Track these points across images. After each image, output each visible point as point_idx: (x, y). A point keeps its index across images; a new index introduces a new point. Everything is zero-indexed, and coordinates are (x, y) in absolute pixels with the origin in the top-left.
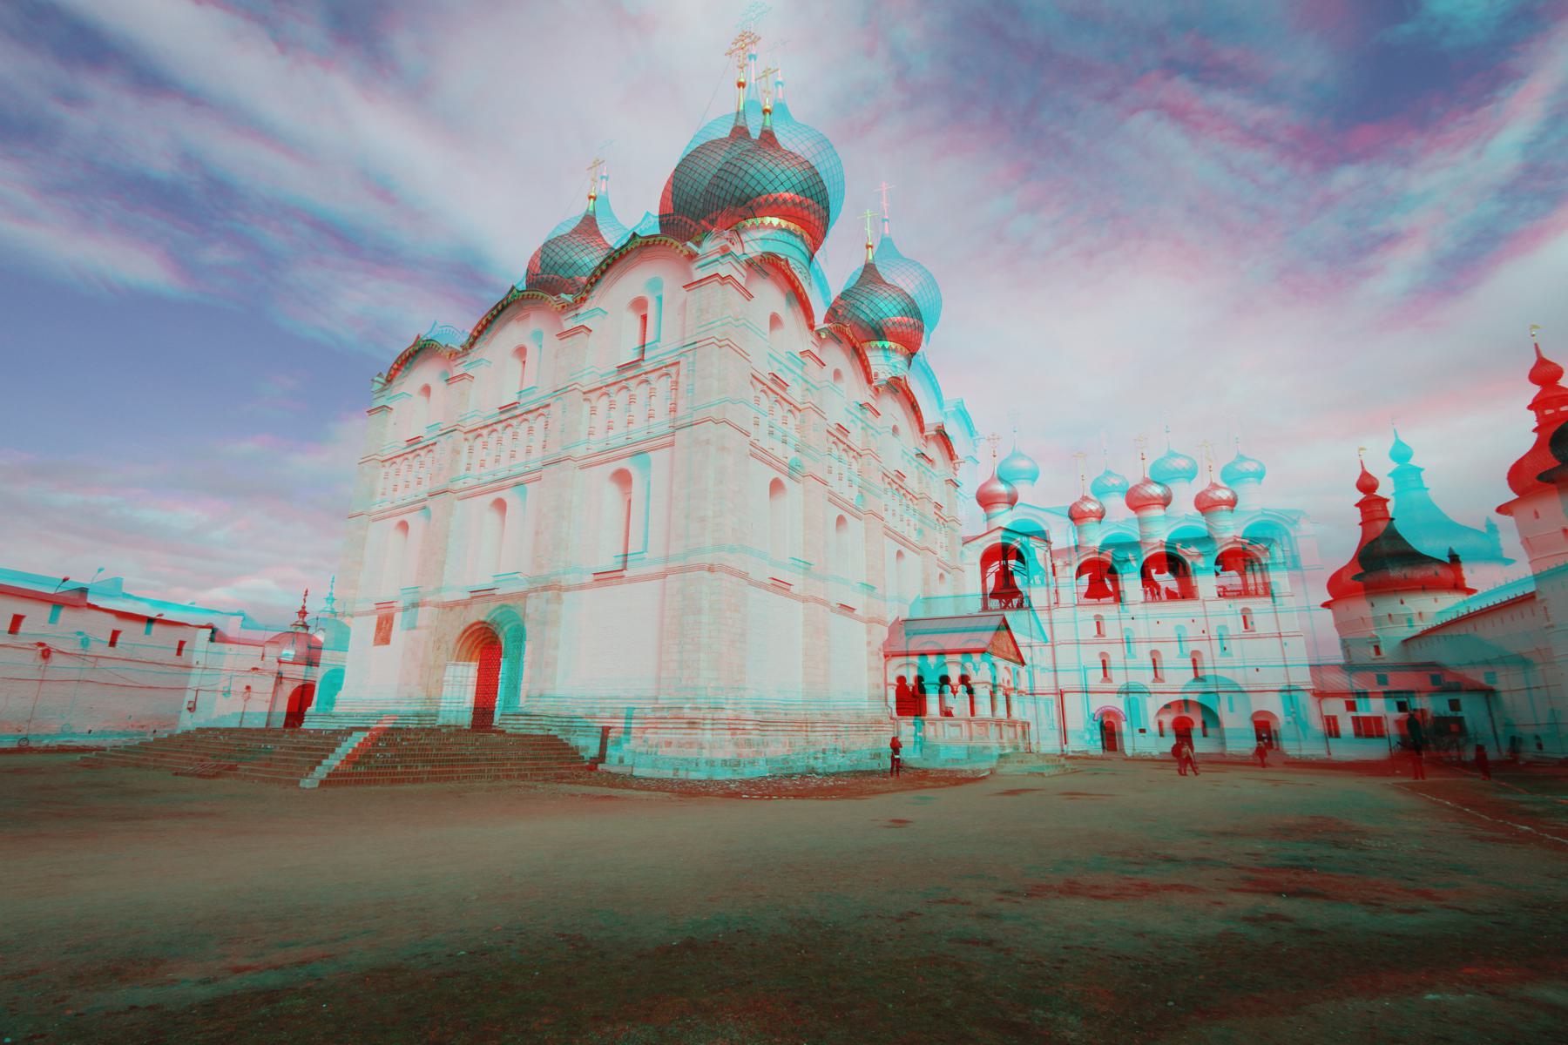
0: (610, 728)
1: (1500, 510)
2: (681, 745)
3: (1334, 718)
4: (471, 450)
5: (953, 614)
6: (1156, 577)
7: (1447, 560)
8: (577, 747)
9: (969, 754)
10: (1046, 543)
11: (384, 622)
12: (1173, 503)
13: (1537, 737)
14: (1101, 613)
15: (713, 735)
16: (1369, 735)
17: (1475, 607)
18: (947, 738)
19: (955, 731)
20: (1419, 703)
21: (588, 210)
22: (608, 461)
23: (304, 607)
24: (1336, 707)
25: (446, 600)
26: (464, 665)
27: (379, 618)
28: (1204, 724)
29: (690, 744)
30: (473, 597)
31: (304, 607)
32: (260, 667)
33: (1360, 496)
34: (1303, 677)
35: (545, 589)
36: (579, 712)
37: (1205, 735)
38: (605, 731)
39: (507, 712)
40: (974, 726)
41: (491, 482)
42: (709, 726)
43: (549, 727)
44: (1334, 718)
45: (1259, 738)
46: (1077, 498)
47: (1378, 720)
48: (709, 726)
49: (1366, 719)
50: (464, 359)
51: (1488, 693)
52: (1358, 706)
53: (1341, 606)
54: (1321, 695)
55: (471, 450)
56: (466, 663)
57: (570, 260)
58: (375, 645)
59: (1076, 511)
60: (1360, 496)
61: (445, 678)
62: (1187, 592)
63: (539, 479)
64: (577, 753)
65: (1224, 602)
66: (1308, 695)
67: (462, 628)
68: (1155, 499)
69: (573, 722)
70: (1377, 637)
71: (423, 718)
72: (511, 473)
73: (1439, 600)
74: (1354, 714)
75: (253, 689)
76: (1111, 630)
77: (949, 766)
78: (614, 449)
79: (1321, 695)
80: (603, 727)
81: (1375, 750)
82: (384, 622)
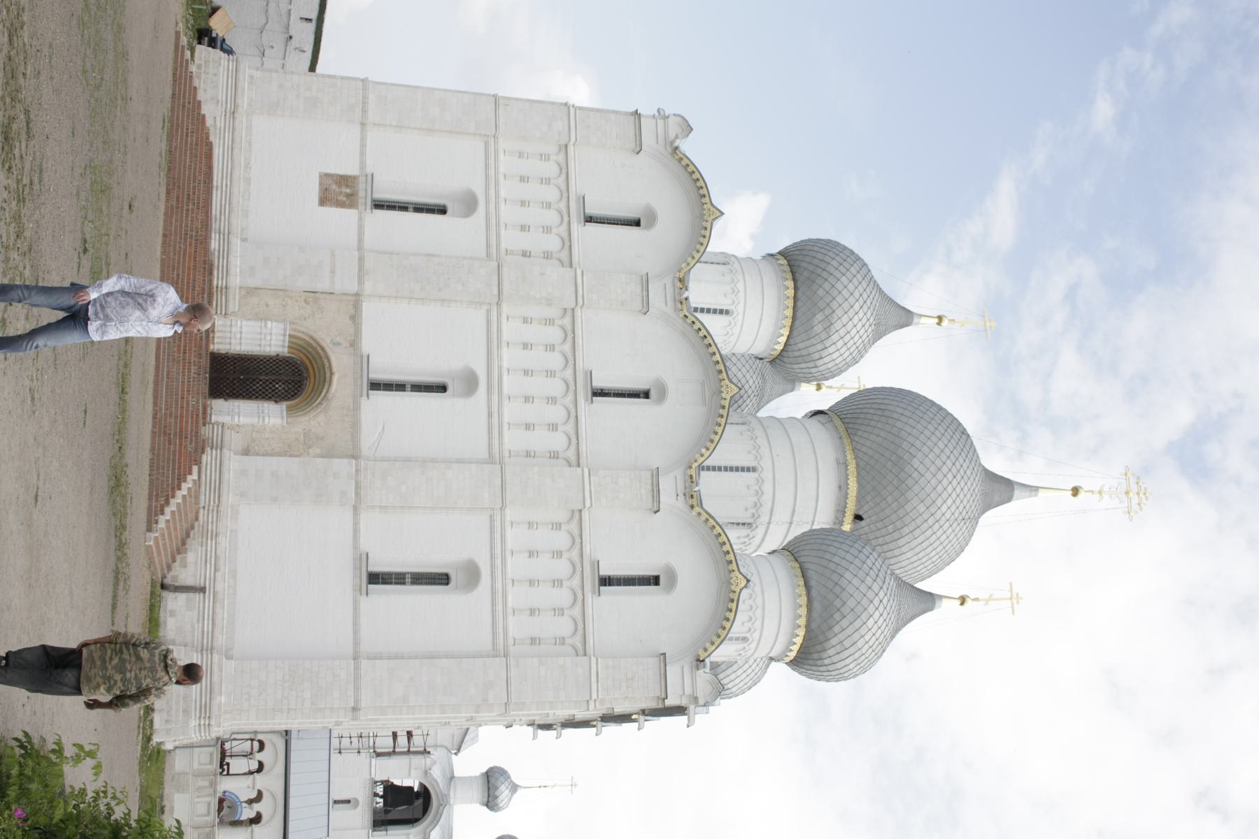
0: (205, 593)
8: (186, 553)
10: (456, 746)
11: (348, 191)
14: (360, 808)
15: (195, 726)
18: (196, 800)
19: (202, 809)
22: (493, 566)
25: (364, 304)
26: (284, 341)
30: (362, 356)
36: (223, 542)
39: (227, 432)
40: (208, 830)
41: (500, 367)
42: (202, 722)
43: (206, 508)
46: (515, 778)
48: (202, 722)
56: (287, 344)
57: (836, 318)
58: (320, 173)
59: (497, 779)
61: (269, 323)
63: (490, 458)
64: (179, 552)
67: (326, 342)
69: (212, 531)
71: (224, 291)
76: (339, 814)
80: (205, 588)
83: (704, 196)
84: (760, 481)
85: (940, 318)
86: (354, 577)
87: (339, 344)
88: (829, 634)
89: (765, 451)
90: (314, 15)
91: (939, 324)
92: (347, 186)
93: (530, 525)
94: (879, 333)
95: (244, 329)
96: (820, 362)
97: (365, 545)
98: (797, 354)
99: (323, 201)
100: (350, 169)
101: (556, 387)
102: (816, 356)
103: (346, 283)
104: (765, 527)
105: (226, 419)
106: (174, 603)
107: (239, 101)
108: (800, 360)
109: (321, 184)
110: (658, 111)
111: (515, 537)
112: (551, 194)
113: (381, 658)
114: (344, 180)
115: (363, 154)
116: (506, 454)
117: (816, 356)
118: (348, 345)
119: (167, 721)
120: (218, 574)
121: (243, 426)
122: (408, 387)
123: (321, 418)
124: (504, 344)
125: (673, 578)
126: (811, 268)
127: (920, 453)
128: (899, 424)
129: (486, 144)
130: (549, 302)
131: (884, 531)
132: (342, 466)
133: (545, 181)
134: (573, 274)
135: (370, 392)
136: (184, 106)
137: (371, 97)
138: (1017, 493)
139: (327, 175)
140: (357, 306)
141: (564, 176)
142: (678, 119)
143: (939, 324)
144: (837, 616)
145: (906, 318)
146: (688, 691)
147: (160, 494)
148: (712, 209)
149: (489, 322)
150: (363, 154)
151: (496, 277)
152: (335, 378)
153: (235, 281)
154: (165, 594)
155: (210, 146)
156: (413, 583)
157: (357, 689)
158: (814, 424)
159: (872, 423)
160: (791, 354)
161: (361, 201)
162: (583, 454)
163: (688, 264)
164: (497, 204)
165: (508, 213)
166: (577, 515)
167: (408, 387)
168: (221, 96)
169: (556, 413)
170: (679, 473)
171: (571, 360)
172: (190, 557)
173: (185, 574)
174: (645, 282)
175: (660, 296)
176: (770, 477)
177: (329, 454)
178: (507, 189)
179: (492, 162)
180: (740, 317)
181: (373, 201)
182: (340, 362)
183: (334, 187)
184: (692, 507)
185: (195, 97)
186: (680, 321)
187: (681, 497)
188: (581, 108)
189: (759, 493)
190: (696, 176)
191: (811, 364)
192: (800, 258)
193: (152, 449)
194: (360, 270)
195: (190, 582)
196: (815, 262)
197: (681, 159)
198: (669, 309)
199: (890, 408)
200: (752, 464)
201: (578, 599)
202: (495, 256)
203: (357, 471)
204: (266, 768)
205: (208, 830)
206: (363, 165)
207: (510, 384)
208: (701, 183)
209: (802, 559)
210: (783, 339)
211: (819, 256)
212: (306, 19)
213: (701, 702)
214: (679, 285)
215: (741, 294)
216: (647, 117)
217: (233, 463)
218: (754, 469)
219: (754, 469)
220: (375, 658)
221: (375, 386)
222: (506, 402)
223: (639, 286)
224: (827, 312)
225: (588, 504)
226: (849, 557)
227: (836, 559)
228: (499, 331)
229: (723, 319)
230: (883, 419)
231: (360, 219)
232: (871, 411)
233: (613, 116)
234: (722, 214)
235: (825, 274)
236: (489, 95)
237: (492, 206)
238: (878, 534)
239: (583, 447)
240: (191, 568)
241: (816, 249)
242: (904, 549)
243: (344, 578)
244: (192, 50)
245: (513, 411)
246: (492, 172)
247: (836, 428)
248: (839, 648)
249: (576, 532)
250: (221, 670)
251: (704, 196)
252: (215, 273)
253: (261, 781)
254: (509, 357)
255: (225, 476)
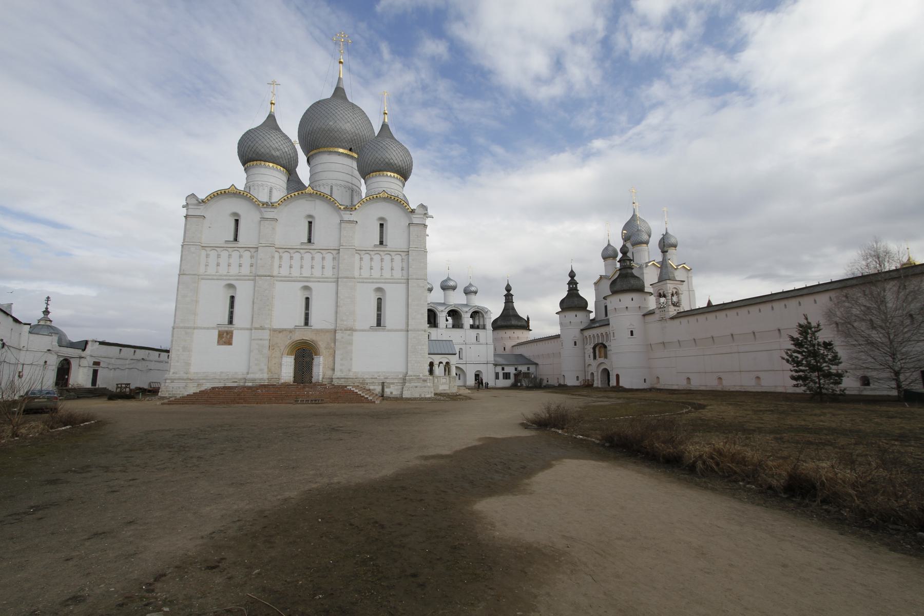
1: (556, 313)
2: (421, 387)
3: (498, 373)
4: (281, 257)
5: (436, 339)
6: (448, 318)
7: (526, 319)
9: (449, 388)
11: (225, 334)
12: (457, 289)
13: (548, 379)
16: (506, 379)
17: (531, 338)
19: (444, 381)
20: (520, 368)
21: (271, 112)
22: (377, 283)
23: (47, 308)
24: (499, 369)
25: (274, 327)
27: (219, 332)
28: (459, 375)
29: (425, 387)
31: (47, 308)
32: (51, 349)
33: (506, 292)
34: (491, 359)
35: (346, 330)
36: (367, 376)
37: (459, 379)
38: (383, 383)
39: (325, 377)
41: (300, 277)
44: (498, 373)
45: (476, 380)
47: (509, 373)
49: (506, 373)
50: (272, 210)
51: (536, 364)
52: (505, 369)
53: (496, 332)
54: (496, 365)
55: (281, 257)
60: (506, 292)
62: (458, 325)
65: (472, 330)
66: (492, 365)
68: (450, 287)
70: (505, 344)
72: (323, 276)
73: (515, 333)
74: (504, 372)
75: (48, 363)
77: (442, 392)
78: (374, 279)
79: (496, 365)
81: (508, 383)
82: (225, 334)
83: (225, 192)
84: (337, 185)
85: (272, 103)
86: (379, 331)
87: (291, 337)
88: (398, 165)
89: (324, 182)
90: (133, 350)
91: (274, 104)
92: (223, 334)
93: (371, 269)
94: (277, 129)
95: (285, 372)
96: (291, 155)
97: (367, 327)
98: (288, 164)
99: (230, 344)
100: (215, 334)
101: (307, 256)
102: (289, 157)
103: (266, 334)
104: (353, 186)
105: (321, 377)
106: (388, 391)
107: (185, 378)
108: (290, 163)
109: (222, 345)
110: (183, 207)
111: (365, 273)
112: (225, 254)
113: (408, 322)
114: (220, 335)
115: (208, 328)
116: (334, 276)
117: (289, 157)
118: (291, 334)
119: (428, 393)
120: (378, 378)
121: (323, 370)
122: (307, 311)
123: (320, 343)
124: (290, 275)
125: (382, 219)
126: (251, 153)
127: (322, 121)
128: (315, 128)
129: (202, 279)
130: (273, 257)
131: (356, 141)
132: (338, 336)
133: (219, 256)
134: (261, 247)
135: (309, 325)
136: (197, 399)
137: (181, 325)
138: (341, 86)
139: (218, 342)
140: (275, 330)
141: (216, 248)
142: (188, 199)
143: (274, 104)
144: (392, 161)
145: (271, 118)
146: (422, 216)
147: (359, 399)
148: (231, 189)
149: (281, 281)
150: (208, 328)
151: (263, 277)
152: (304, 338)
153: (265, 376)
154: (385, 396)
155: (213, 388)
156: (381, 311)
157: (418, 330)
158: (313, 162)
159: (314, 139)
160: (288, 167)
161: (230, 329)
162: (335, 248)
163: (256, 201)
164: (230, 276)
165: (234, 270)
166: (358, 251)
167: (307, 311)
168: (184, 385)
169: (318, 256)
170: (342, 213)
171: (297, 250)
172: (372, 387)
173: (378, 389)
174: (263, 219)
175: (270, 213)
176: (334, 181)
177: (335, 341)
178: (223, 270)
179: (210, 277)
180: (273, 184)
181: (228, 325)
182: (298, 336)
183: (223, 340)
184: (356, 209)
185: (192, 395)
186: (281, 206)
187: (351, 213)
188: (184, 240)
189: (341, 186)
190: (215, 194)
191: (292, 159)
192: (247, 157)
193: (344, 403)
194: (260, 329)
195: (380, 387)
196: (249, 151)
197: (208, 199)
198: (276, 210)
199: (308, 131)
200: (329, 187)
201: (389, 253)
202: (255, 277)
203: (341, 330)
204: (432, 361)
205: (451, 379)
206: (213, 328)
207: (306, 273)
208: (219, 192)
209: (369, 171)
210: (282, 169)
211: (246, 149)
212: (134, 353)
213: (426, 212)
214: (265, 206)
215: (263, 183)
216: (187, 212)
217: (338, 374)
218: (332, 187)
219: (332, 187)
220: (408, 324)
221: (306, 323)
222: (313, 276)
223: (266, 221)
224: (271, 149)
225: (354, 247)
226: (369, 154)
227: (370, 158)
228: (285, 277)
229: (274, 191)
230: (313, 134)
231: (238, 329)
232: (309, 138)
233: (187, 226)
234: (233, 185)
235: (255, 148)
236: (179, 278)
237: (231, 278)
238: (357, 143)
239: (332, 248)
240: (376, 387)
241: (243, 150)
242: (363, 133)
243: (380, 335)
244: (163, 398)
245: (317, 272)
246: (215, 277)
247: (315, 154)
248: (403, 162)
249: (364, 252)
250: (411, 376)
251: (225, 192)
252: (262, 383)
253: (436, 363)
254: (295, 272)
255: (343, 376)
